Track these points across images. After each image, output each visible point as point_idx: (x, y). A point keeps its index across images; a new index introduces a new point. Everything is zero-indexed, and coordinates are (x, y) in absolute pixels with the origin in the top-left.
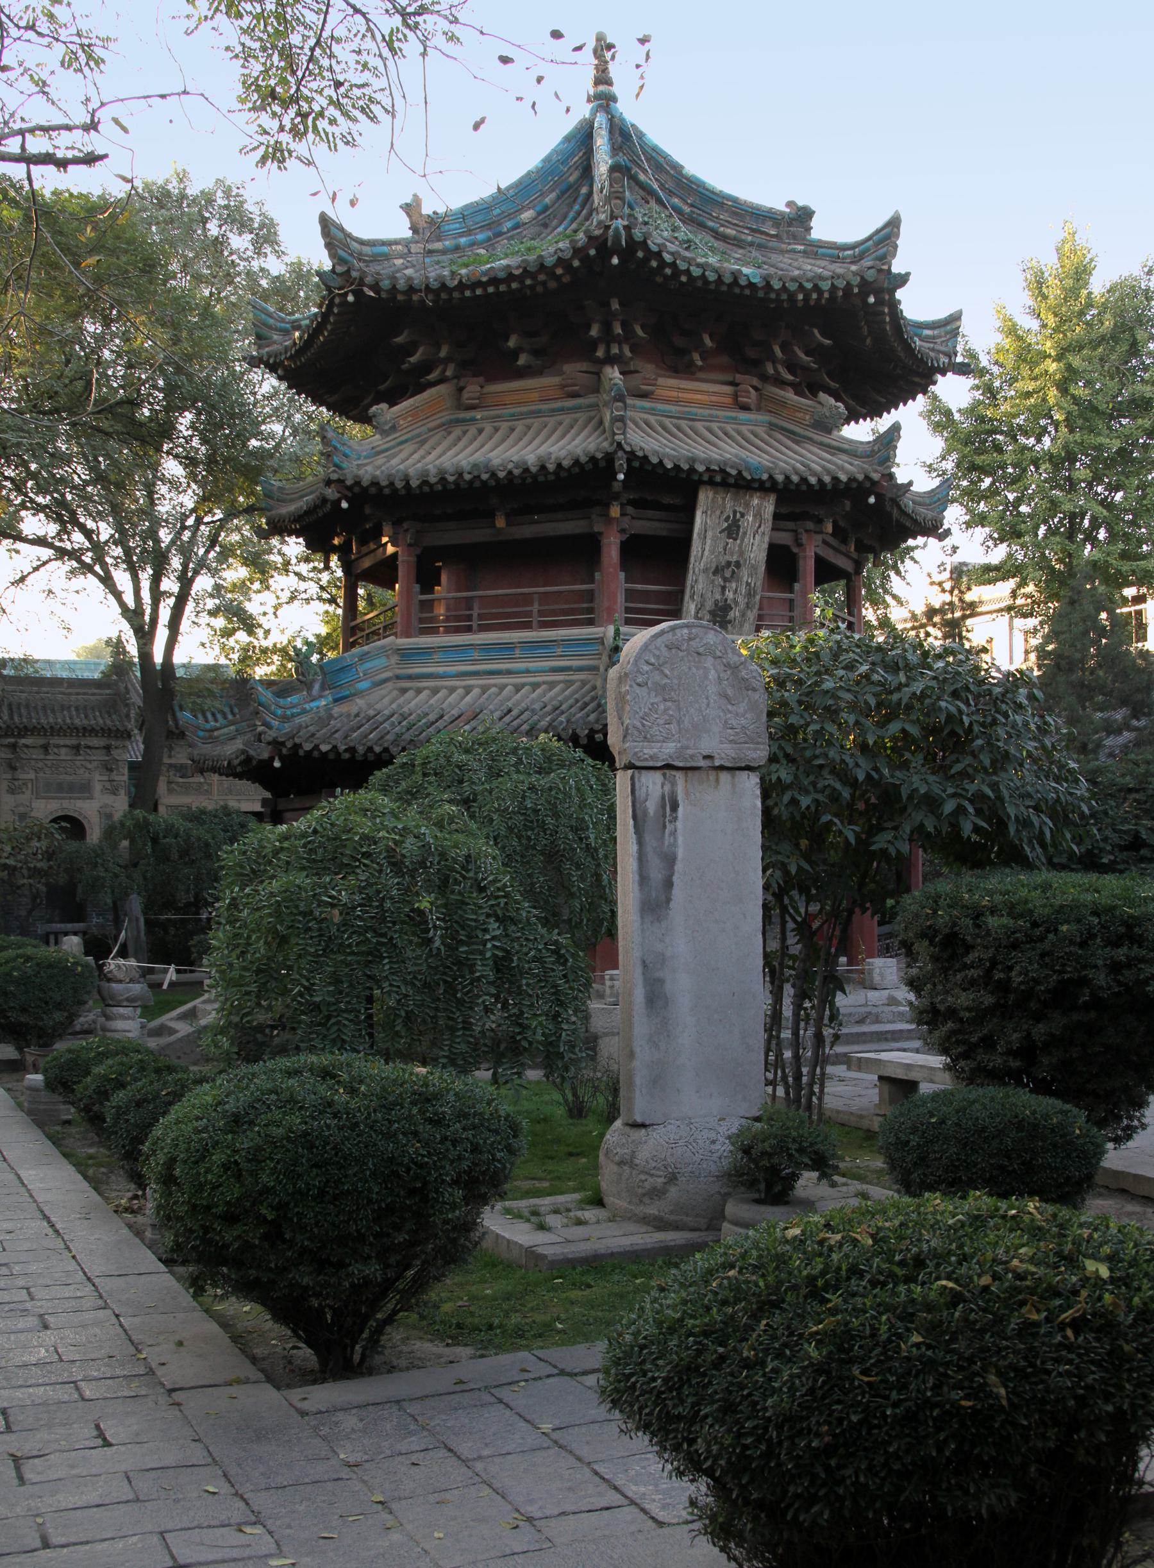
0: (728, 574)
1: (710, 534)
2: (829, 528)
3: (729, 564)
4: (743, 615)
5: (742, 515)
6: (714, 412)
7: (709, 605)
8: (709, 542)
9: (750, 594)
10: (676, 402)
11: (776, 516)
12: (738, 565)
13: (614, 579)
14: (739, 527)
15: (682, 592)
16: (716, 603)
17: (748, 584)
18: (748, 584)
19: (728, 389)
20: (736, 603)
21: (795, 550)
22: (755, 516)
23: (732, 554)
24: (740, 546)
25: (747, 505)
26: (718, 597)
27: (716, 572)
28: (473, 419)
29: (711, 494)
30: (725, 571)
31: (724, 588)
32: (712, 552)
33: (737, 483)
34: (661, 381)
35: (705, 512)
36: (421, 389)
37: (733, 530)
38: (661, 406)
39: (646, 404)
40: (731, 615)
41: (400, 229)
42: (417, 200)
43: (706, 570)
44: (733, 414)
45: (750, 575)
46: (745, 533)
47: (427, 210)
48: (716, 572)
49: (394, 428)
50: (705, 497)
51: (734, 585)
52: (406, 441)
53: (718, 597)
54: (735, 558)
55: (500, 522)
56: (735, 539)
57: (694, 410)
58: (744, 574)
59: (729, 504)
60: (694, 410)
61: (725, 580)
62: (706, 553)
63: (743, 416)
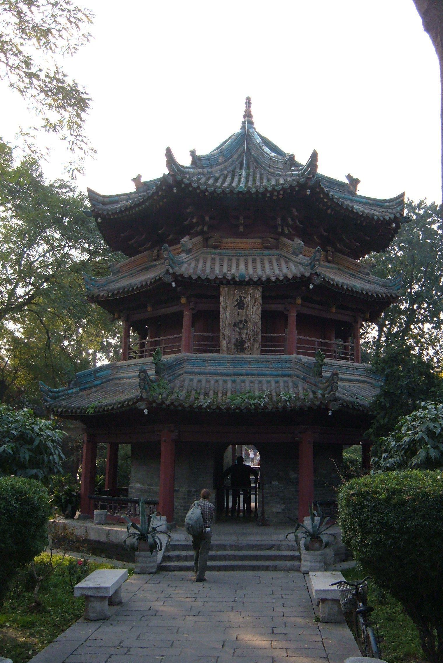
0: (241, 326)
1: (229, 308)
2: (299, 301)
3: (241, 321)
4: (253, 345)
5: (245, 298)
6: (251, 252)
7: (233, 341)
8: (229, 311)
9: (255, 335)
10: (232, 249)
11: (264, 297)
12: (246, 321)
13: (187, 332)
14: (244, 304)
15: (219, 336)
16: (237, 340)
17: (253, 330)
18: (253, 330)
19: (259, 240)
20: (248, 339)
21: (286, 313)
22: (251, 298)
23: (242, 316)
24: (246, 312)
25: (246, 293)
26: (238, 337)
27: (235, 325)
28: (156, 265)
29: (226, 289)
30: (240, 324)
31: (240, 333)
32: (231, 316)
33: (240, 284)
34: (225, 240)
35: (225, 298)
36: (138, 252)
37: (241, 305)
38: (223, 251)
39: (217, 251)
40: (246, 345)
41: (131, 188)
42: (139, 177)
43: (229, 325)
44: (262, 252)
45: (253, 326)
46: (247, 306)
47: (143, 180)
48: (235, 325)
49: (119, 271)
50: (224, 291)
51: (245, 331)
52: (125, 277)
53: (238, 337)
54: (244, 319)
55: (149, 309)
56: (243, 309)
57: (239, 251)
58: (251, 326)
59: (237, 293)
60: (239, 251)
61: (240, 329)
62: (228, 317)
63: (266, 252)
